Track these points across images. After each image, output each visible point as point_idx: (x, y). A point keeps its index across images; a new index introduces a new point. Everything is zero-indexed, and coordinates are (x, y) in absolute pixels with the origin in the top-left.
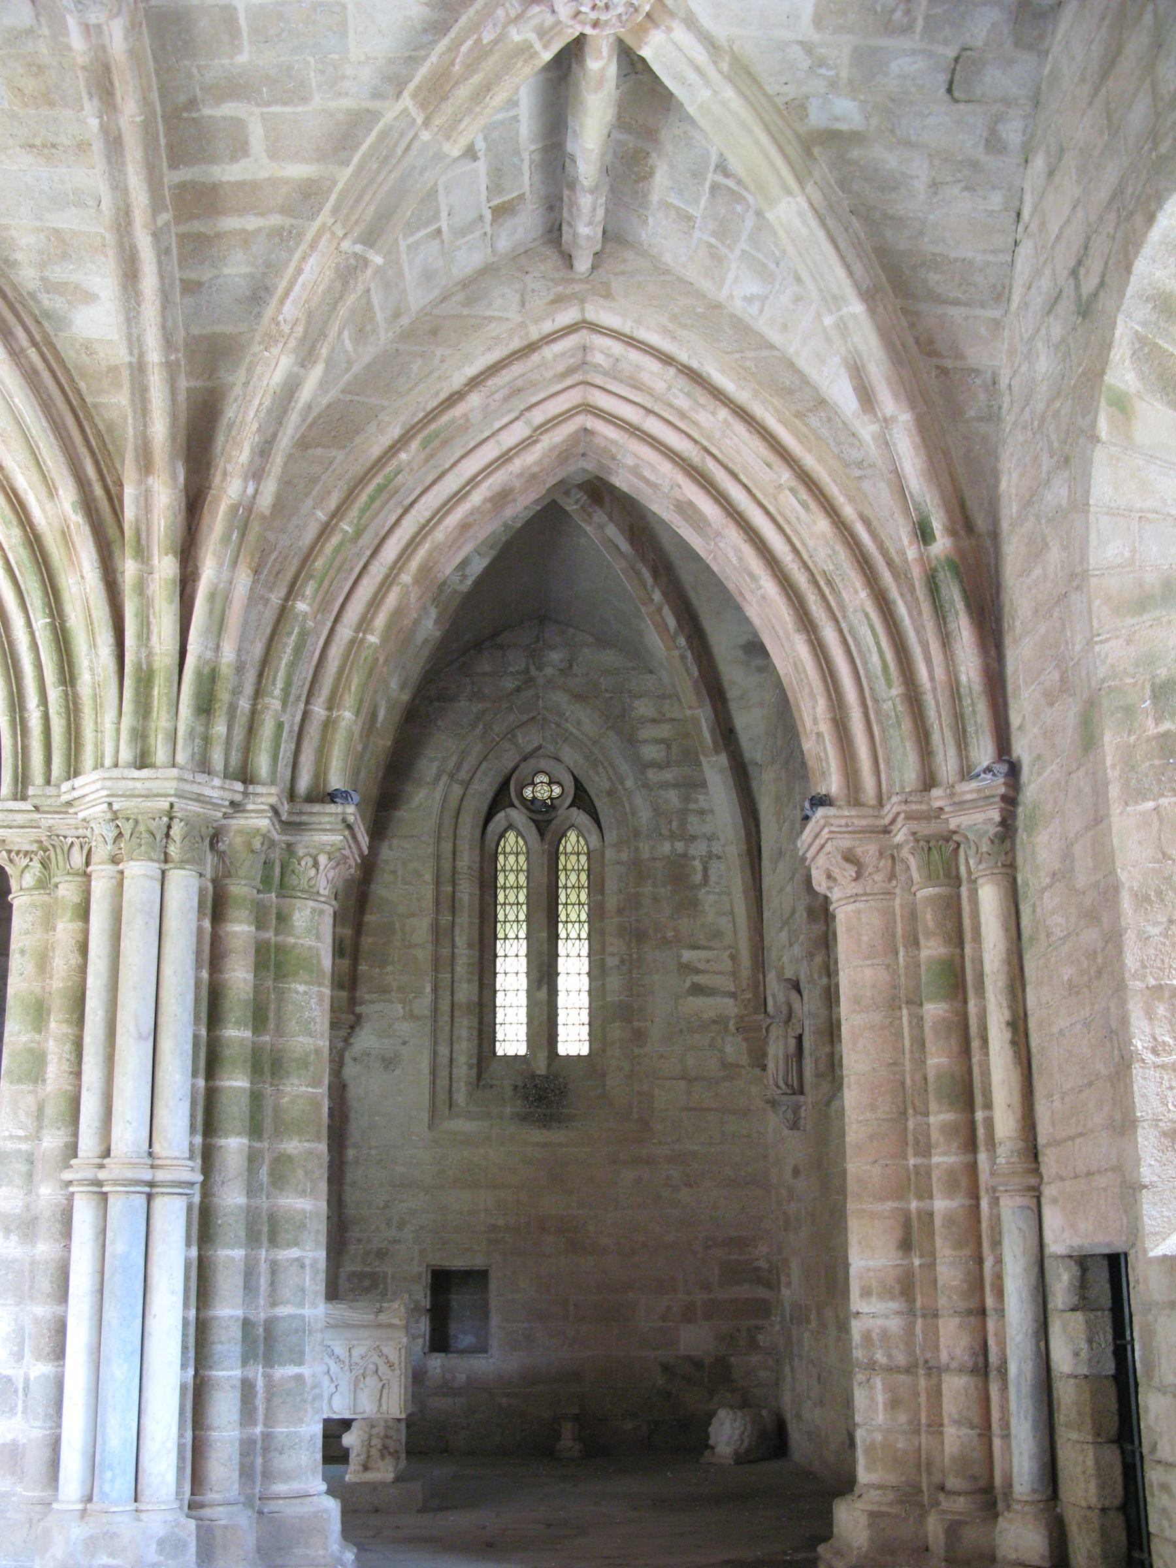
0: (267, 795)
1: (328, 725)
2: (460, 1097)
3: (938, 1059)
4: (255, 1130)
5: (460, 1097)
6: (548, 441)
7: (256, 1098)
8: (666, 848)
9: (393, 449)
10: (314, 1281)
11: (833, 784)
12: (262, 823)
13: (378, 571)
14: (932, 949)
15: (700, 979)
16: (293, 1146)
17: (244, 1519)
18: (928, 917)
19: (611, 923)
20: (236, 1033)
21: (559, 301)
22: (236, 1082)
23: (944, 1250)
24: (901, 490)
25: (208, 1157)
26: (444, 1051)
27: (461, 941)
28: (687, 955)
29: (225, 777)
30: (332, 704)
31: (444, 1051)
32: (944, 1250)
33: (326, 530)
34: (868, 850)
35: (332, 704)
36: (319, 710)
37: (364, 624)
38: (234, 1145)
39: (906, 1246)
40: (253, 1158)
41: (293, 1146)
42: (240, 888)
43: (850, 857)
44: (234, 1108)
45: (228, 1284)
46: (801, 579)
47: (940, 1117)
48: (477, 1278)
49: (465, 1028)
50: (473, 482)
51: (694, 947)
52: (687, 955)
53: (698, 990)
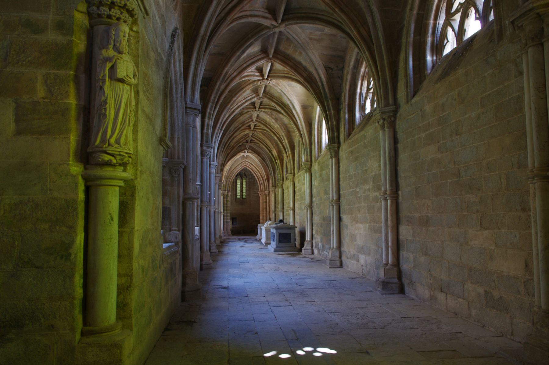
0: (227, 192)
1: (230, 186)
2: (234, 202)
3: (265, 207)
4: (226, 210)
5: (234, 202)
6: (243, 168)
7: (226, 209)
8: (253, 180)
9: (233, 169)
10: (229, 219)
11: (260, 190)
12: (226, 193)
13: (232, 176)
14: (265, 200)
15: (256, 192)
16: (228, 211)
17: (226, 232)
18: (265, 198)
19: (248, 185)
20: (225, 205)
21: (244, 159)
22: (225, 208)
23: (265, 217)
24: (264, 175)
25: (224, 212)
26: (233, 198)
27: (234, 188)
28: (254, 190)
29: (223, 191)
30: (230, 185)
31: (233, 198)
32: (265, 217)
33: (229, 175)
34: (262, 194)
35: (230, 185)
36: (229, 185)
37: (232, 180)
38: (225, 211)
39: (263, 217)
40: (226, 212)
41: (228, 211)
42: (225, 197)
43: (261, 194)
44: (225, 209)
45: (225, 219)
46: (258, 177)
47: (265, 210)
48: (236, 218)
49: (234, 196)
50: (238, 170)
51: (255, 189)
52: (254, 190)
53: (255, 193)
